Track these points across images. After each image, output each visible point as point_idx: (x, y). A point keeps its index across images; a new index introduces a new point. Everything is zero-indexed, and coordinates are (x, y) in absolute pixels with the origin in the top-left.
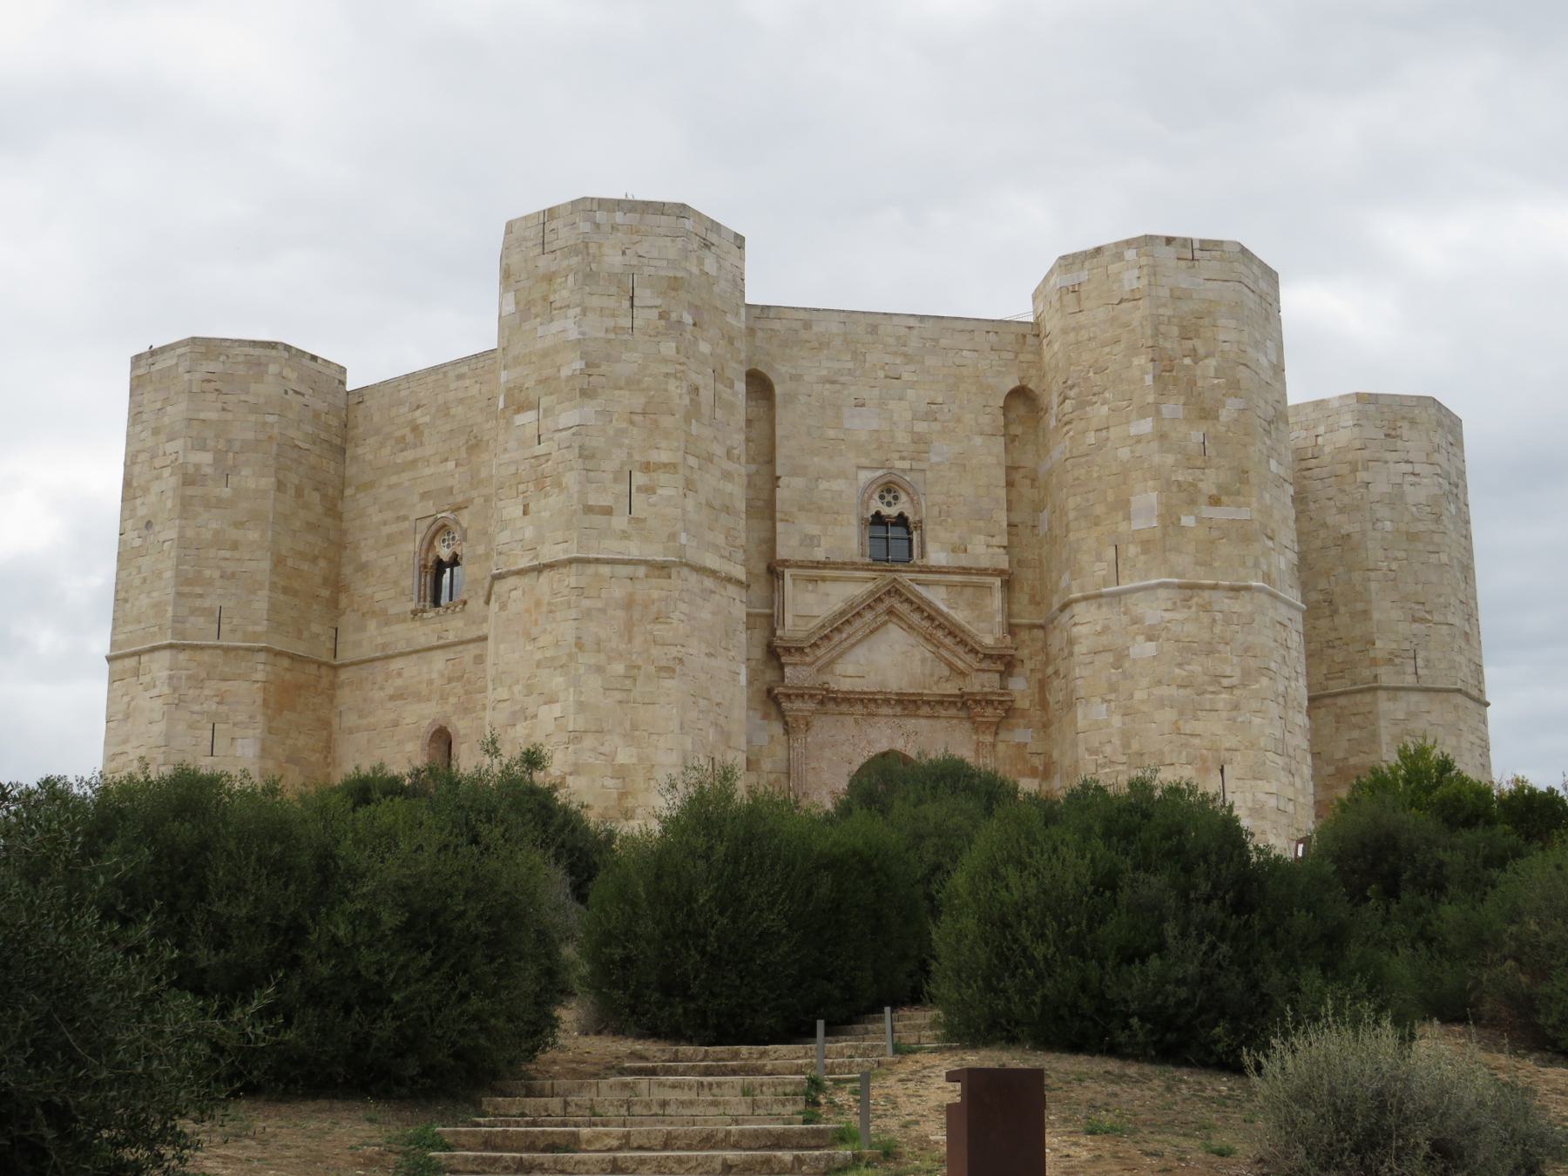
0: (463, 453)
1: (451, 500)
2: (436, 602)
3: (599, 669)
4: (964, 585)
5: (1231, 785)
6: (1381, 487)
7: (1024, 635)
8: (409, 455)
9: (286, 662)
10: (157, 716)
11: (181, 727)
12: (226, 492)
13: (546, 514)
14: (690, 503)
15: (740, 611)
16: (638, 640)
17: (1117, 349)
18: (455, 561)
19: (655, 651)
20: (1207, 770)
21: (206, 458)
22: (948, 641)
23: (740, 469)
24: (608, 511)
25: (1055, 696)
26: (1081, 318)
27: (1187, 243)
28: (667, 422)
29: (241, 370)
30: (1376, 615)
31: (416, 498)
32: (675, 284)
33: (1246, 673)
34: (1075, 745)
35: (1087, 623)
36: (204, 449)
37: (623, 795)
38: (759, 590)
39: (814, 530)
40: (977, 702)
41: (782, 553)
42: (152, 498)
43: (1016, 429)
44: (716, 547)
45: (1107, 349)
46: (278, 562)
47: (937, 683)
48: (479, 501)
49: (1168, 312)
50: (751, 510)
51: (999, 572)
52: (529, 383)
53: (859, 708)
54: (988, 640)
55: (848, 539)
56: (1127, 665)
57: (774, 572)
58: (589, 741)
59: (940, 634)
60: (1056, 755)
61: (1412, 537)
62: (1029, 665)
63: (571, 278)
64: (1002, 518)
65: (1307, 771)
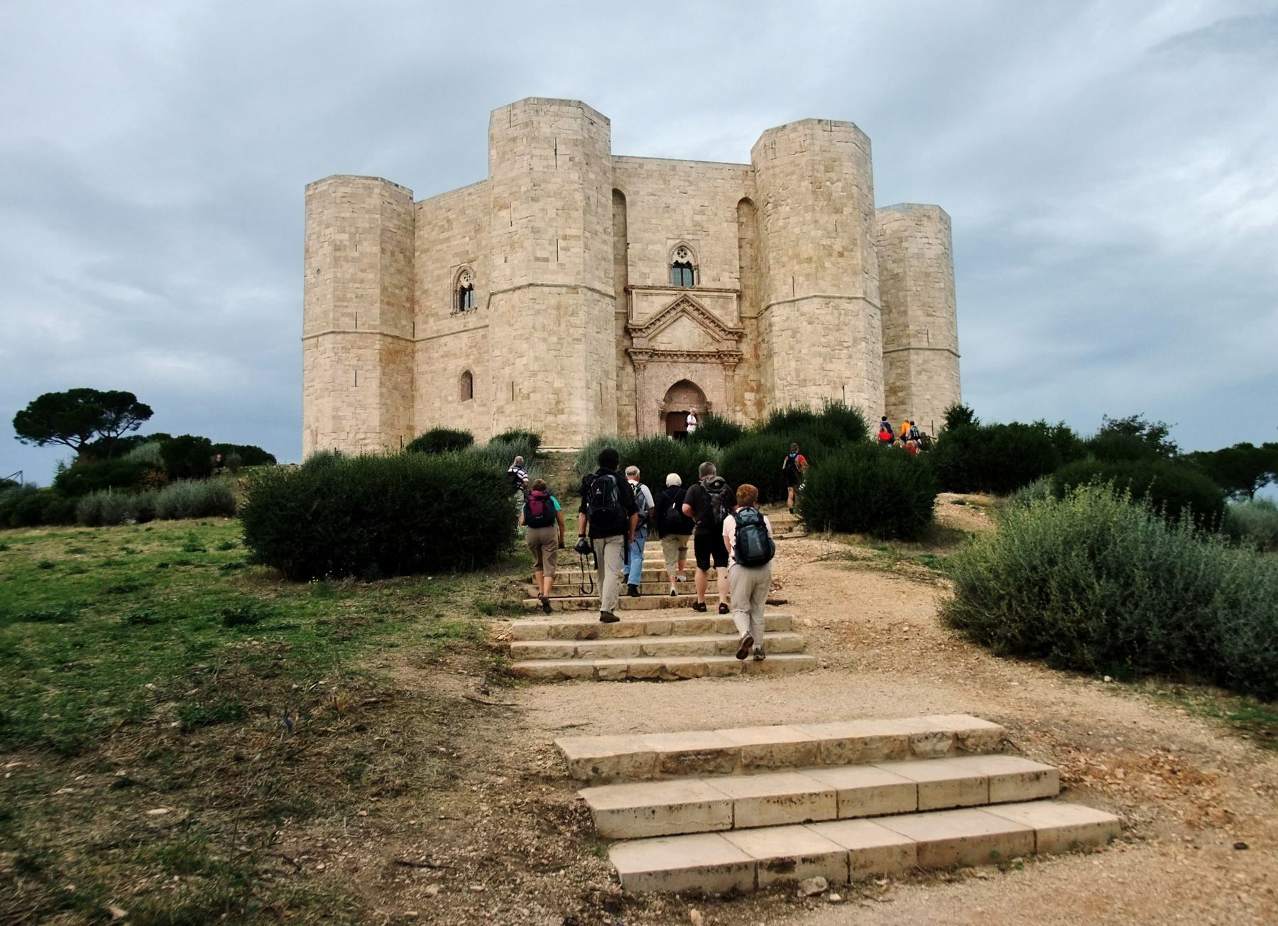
2: (462, 309)
3: (545, 340)
4: (719, 297)
5: (847, 395)
6: (913, 250)
7: (747, 322)
8: (446, 235)
9: (390, 340)
10: (328, 367)
11: (340, 372)
12: (356, 254)
14: (587, 255)
15: (612, 310)
16: (563, 325)
17: (794, 177)
18: (471, 288)
19: (571, 330)
20: (836, 388)
21: (345, 237)
22: (712, 325)
23: (611, 239)
24: (547, 260)
25: (763, 351)
26: (776, 162)
27: (830, 123)
28: (575, 214)
29: (361, 191)
30: (910, 313)
31: (449, 257)
32: (575, 143)
33: (855, 340)
34: (773, 375)
35: (779, 316)
36: (344, 232)
37: (558, 403)
38: (621, 300)
39: (647, 270)
41: (631, 282)
42: (319, 258)
43: (743, 219)
44: (600, 278)
46: (384, 289)
49: (819, 158)
50: (616, 261)
51: (736, 291)
52: (506, 195)
54: (731, 325)
55: (662, 274)
56: (798, 335)
57: (627, 291)
58: (540, 376)
59: (707, 321)
60: (763, 381)
61: (927, 275)
62: (750, 337)
64: (737, 263)
65: (882, 388)
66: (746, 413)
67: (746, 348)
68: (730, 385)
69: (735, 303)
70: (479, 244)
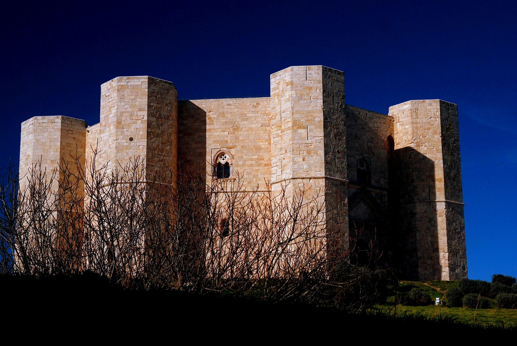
0: (231, 130)
1: (227, 145)
13: (312, 162)
17: (430, 131)
18: (227, 163)
21: (154, 119)
26: (418, 120)
45: (426, 131)
48: (239, 148)
63: (318, 90)
70: (237, 138)
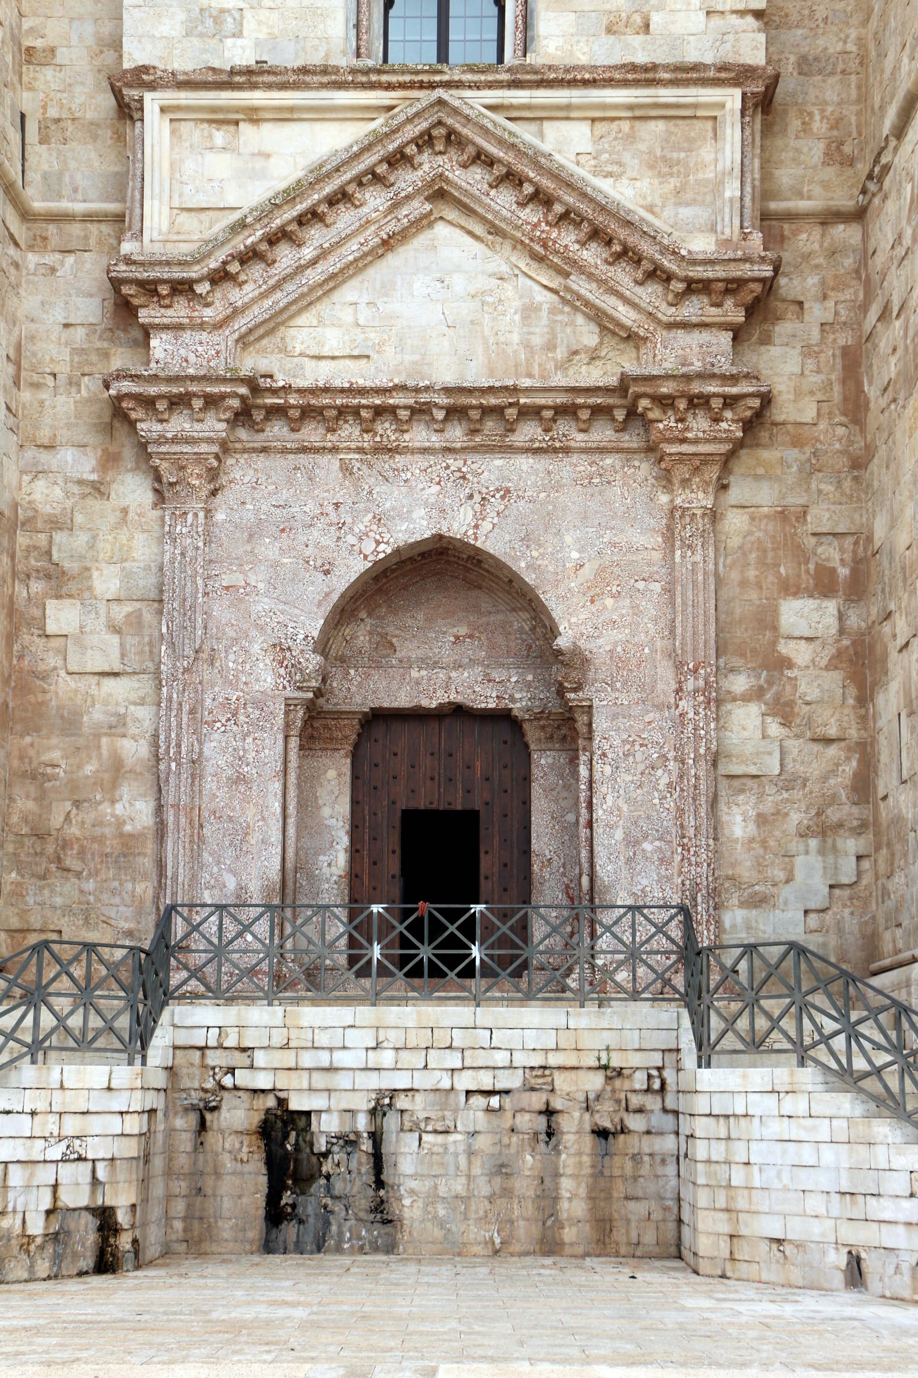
40: (665, 402)
47: (563, 366)
53: (349, 432)
59: (567, 238)
62: (817, 312)
66: (783, 710)
67: (788, 367)
68: (695, 560)
69: (732, 134)
